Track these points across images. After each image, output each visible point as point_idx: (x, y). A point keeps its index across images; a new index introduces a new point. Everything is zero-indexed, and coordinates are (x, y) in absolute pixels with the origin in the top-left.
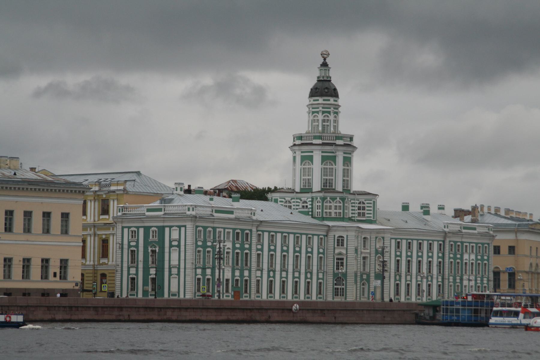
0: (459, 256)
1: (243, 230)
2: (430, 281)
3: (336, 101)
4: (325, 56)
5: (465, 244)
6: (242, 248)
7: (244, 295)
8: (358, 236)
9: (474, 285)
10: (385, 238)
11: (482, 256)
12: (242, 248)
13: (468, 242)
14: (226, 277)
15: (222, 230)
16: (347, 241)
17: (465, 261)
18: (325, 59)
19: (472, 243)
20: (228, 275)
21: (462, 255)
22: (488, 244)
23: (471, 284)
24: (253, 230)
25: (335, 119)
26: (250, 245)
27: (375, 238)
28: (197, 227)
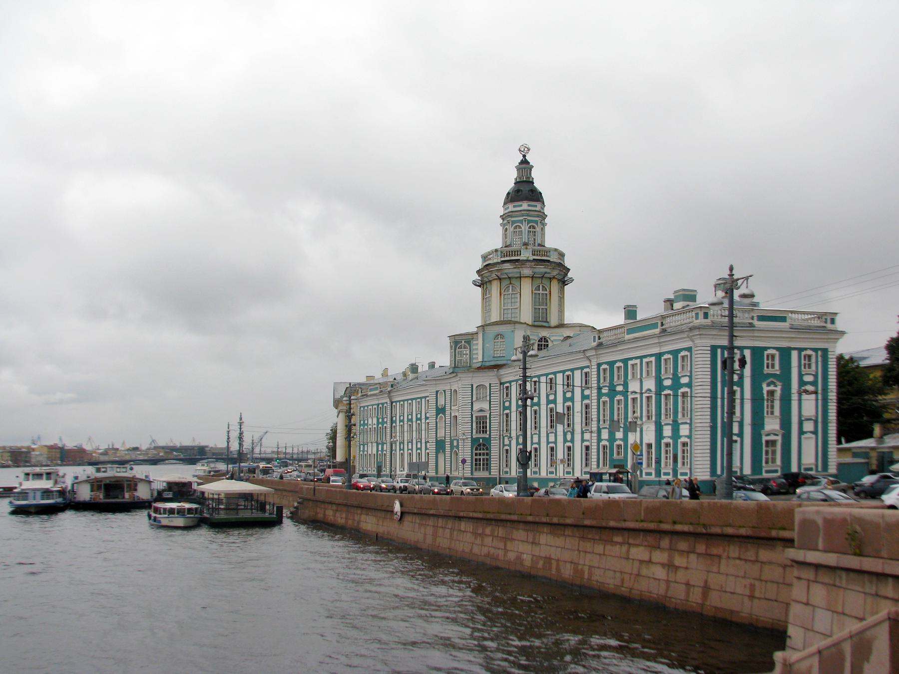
2: (569, 442)
3: (521, 206)
4: (524, 151)
5: (630, 362)
6: (383, 423)
9: (652, 440)
11: (676, 378)
13: (636, 358)
15: (371, 407)
17: (630, 397)
18: (524, 156)
19: (645, 356)
20: (375, 452)
21: (625, 385)
22: (689, 349)
23: (646, 441)
25: (518, 230)
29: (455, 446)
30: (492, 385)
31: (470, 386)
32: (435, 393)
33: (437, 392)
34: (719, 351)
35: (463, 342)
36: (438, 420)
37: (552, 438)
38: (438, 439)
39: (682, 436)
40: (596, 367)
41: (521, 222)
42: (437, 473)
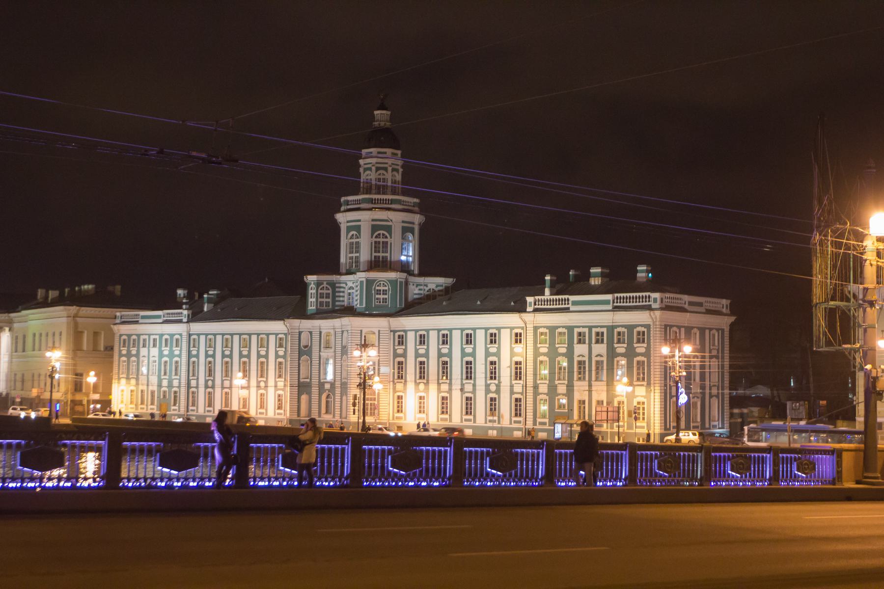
0: (563, 350)
1: (172, 336)
5: (576, 330)
7: (173, 408)
8: (311, 333)
10: (349, 332)
12: (171, 355)
13: (583, 327)
14: (151, 388)
15: (147, 337)
16: (320, 340)
17: (576, 359)
22: (648, 327)
24: (183, 334)
26: (181, 351)
27: (341, 332)
28: (121, 335)
29: (327, 390)
30: (381, 332)
31: (359, 332)
32: (298, 334)
33: (300, 333)
34: (668, 328)
35: (325, 283)
36: (301, 362)
37: (469, 387)
38: (302, 380)
39: (638, 396)
40: (533, 329)
41: (386, 169)
42: (299, 415)
